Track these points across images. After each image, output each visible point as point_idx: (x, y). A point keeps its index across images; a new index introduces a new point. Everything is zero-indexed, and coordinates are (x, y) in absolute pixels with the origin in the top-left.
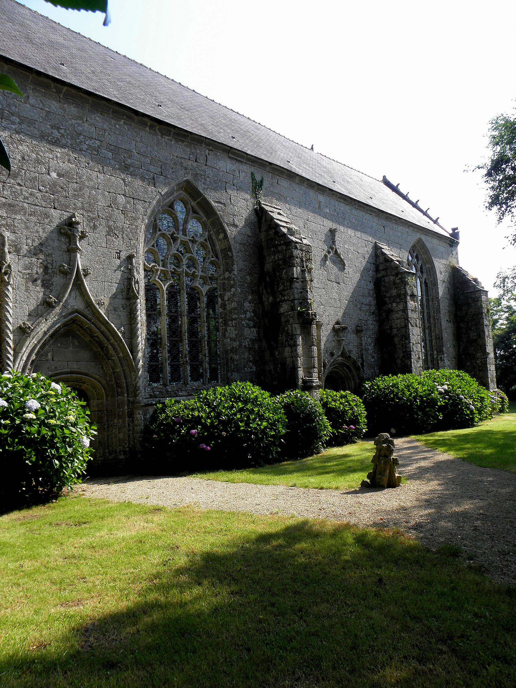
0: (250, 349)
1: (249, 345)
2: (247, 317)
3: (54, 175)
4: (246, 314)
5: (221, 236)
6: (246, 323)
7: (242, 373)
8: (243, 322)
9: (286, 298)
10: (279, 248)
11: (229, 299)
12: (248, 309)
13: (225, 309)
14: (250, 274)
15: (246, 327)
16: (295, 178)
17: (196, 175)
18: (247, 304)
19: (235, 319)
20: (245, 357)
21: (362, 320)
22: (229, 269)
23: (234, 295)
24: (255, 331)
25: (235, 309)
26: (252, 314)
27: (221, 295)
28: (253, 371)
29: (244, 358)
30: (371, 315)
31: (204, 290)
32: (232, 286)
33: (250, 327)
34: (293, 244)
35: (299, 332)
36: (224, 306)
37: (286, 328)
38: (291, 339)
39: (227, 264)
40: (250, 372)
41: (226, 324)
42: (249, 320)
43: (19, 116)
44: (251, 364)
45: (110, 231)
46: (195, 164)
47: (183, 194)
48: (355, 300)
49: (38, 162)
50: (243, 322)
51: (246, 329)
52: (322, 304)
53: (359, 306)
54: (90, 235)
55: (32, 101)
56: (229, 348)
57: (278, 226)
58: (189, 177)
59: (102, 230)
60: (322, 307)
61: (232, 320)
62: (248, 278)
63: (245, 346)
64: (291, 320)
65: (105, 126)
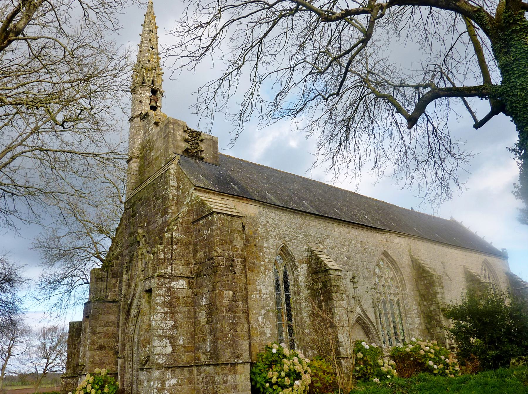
3: (345, 258)
5: (399, 273)
9: (434, 302)
10: (427, 278)
11: (406, 304)
13: (405, 309)
14: (413, 291)
17: (387, 248)
18: (414, 306)
19: (410, 314)
22: (404, 289)
23: (408, 302)
25: (410, 309)
27: (402, 302)
31: (396, 299)
32: (407, 298)
34: (434, 276)
35: (443, 319)
36: (404, 307)
37: (436, 318)
38: (440, 323)
39: (403, 287)
41: (406, 317)
43: (334, 237)
45: (364, 278)
46: (386, 243)
47: (382, 256)
49: (341, 254)
51: (416, 319)
55: (336, 230)
56: (409, 328)
57: (424, 267)
58: (385, 249)
61: (409, 314)
62: (412, 293)
64: (438, 314)
65: (357, 234)
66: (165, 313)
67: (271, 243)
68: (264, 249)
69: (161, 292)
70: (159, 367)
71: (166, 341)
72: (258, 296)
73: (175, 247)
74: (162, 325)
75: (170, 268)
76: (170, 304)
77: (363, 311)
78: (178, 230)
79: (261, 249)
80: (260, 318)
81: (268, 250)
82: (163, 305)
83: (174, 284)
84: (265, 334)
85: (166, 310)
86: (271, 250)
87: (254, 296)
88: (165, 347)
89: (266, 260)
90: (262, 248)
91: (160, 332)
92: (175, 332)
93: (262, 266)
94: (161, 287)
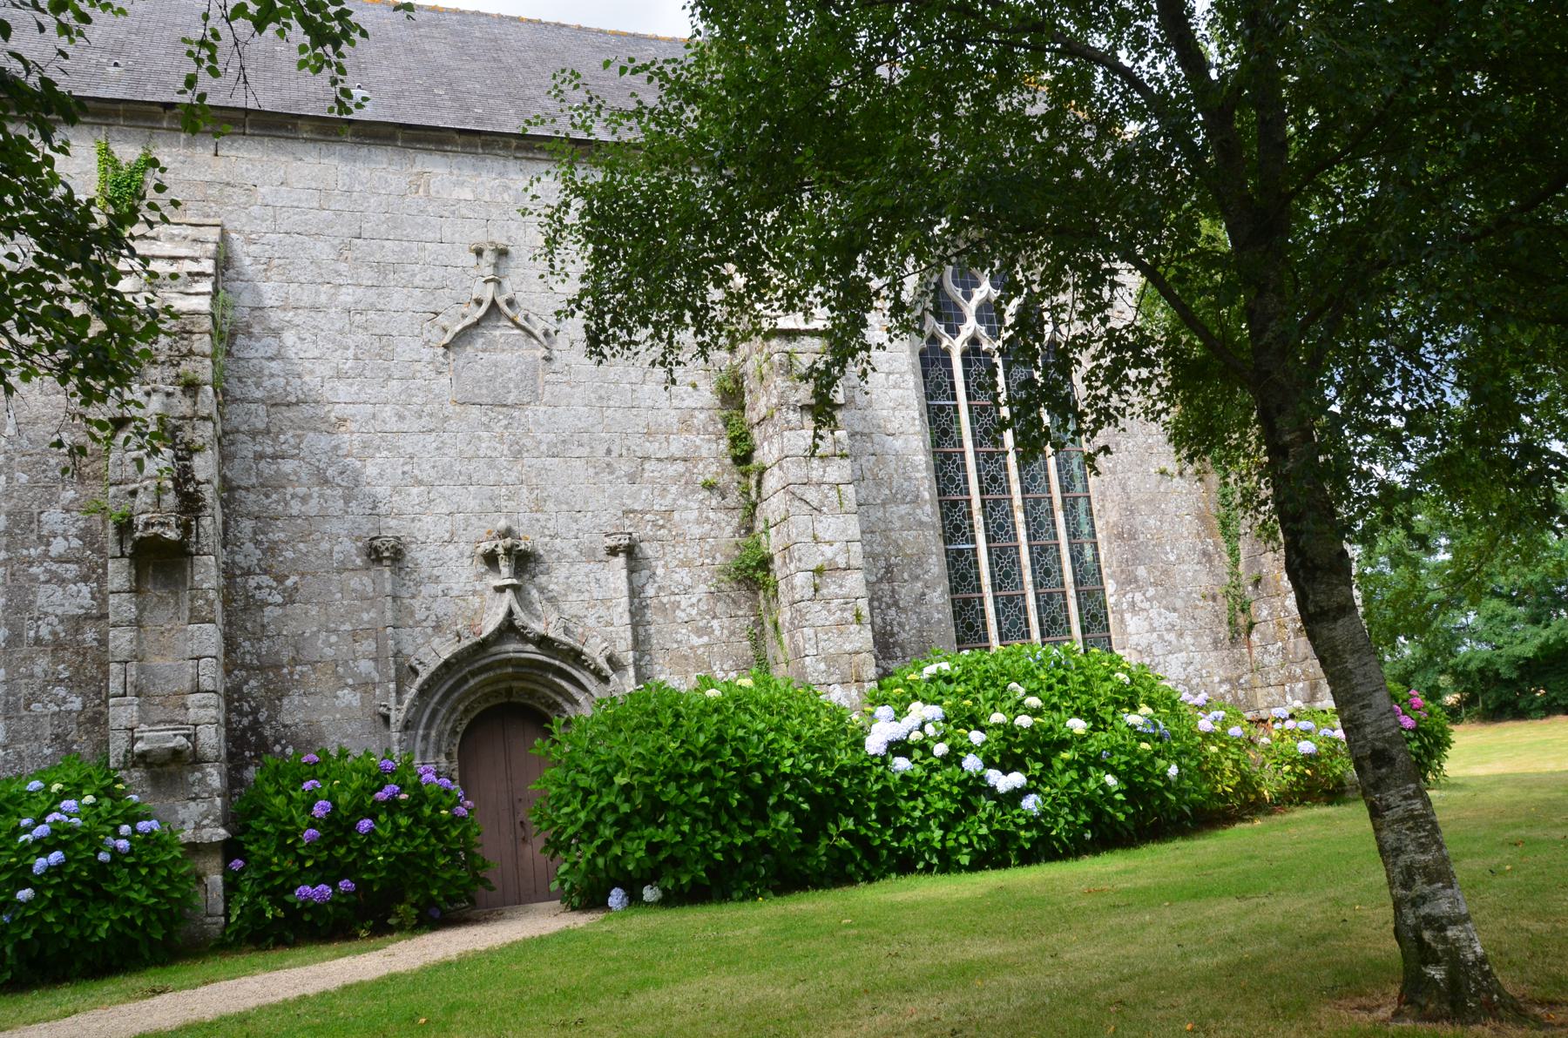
0: (58, 646)
1: (54, 633)
2: (53, 553)
4: (48, 544)
6: (46, 571)
7: (21, 719)
8: (34, 570)
12: (59, 528)
15: (47, 582)
16: (295, 125)
20: (38, 670)
21: (644, 512)
24: (85, 590)
26: (76, 543)
28: (70, 712)
29: (32, 676)
30: (694, 492)
33: (62, 581)
40: (54, 714)
42: (61, 560)
44: (61, 691)
48: (601, 451)
50: (34, 570)
52: (420, 483)
53: (624, 467)
60: (415, 490)
63: (38, 641)
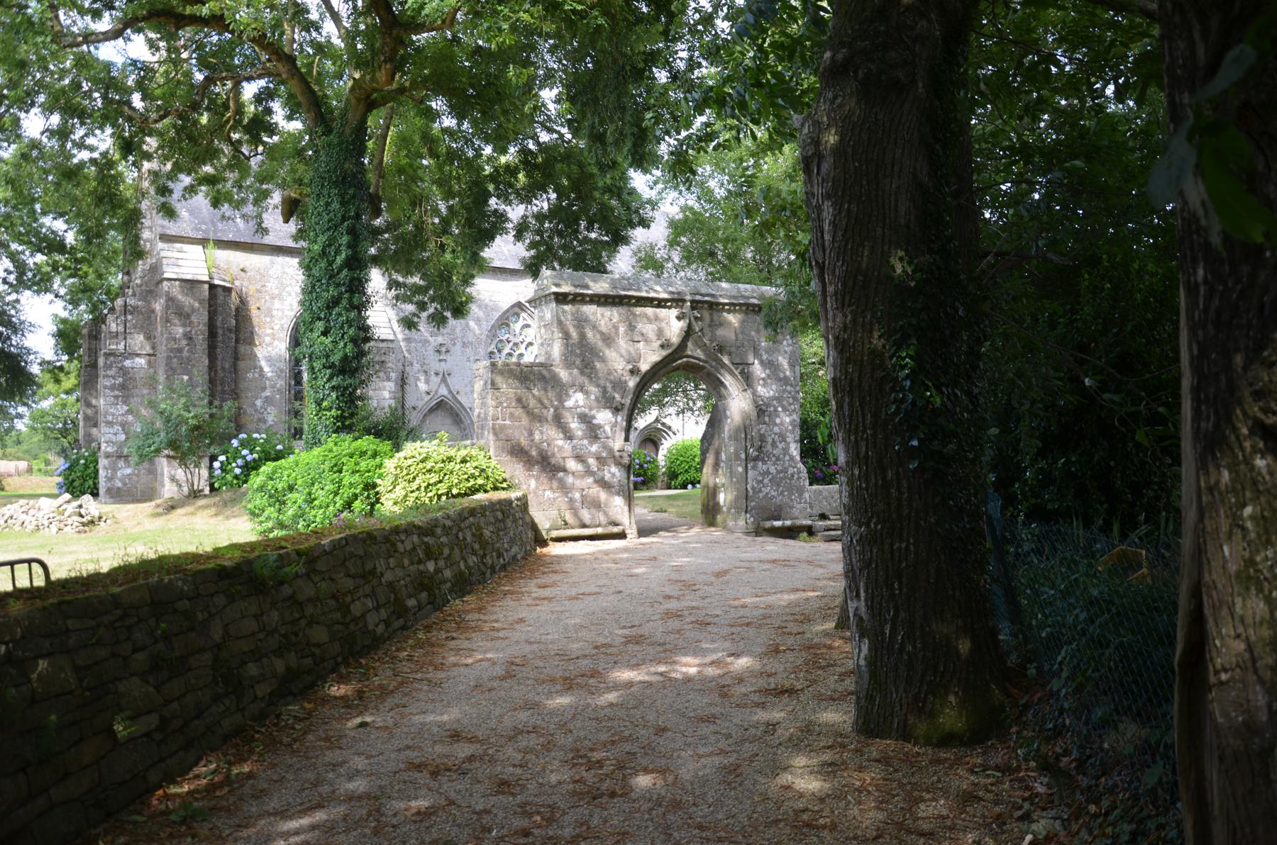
45: (464, 345)
54: (453, 349)
59: (459, 345)
66: (116, 397)
67: (287, 303)
68: (275, 312)
69: (109, 373)
70: (108, 456)
71: (118, 428)
72: (257, 375)
73: (129, 317)
74: (112, 410)
75: (123, 343)
76: (123, 387)
77: (450, 392)
78: (134, 295)
79: (269, 313)
80: (259, 403)
81: (280, 313)
82: (112, 388)
83: (128, 363)
84: (265, 421)
85: (117, 393)
86: (286, 313)
87: (250, 375)
88: (115, 434)
89: (276, 327)
90: (270, 310)
91: (110, 418)
92: (130, 418)
93: (268, 335)
94: (110, 367)
